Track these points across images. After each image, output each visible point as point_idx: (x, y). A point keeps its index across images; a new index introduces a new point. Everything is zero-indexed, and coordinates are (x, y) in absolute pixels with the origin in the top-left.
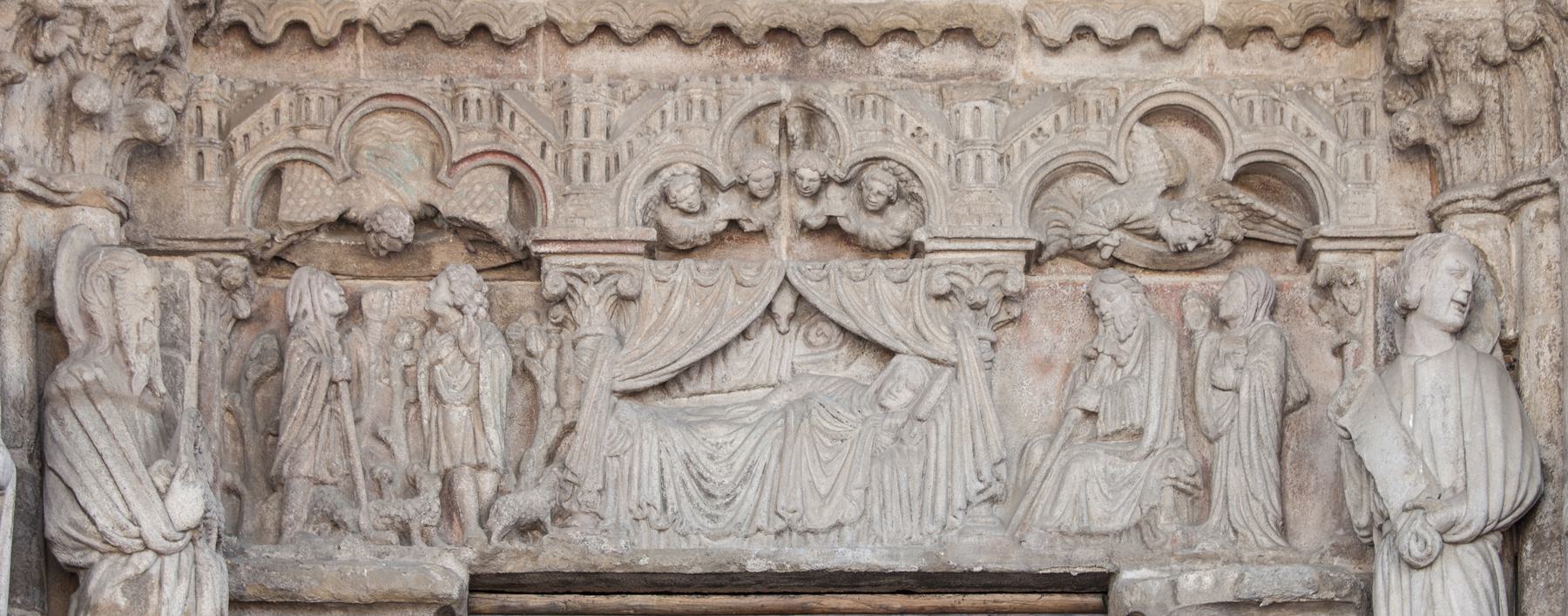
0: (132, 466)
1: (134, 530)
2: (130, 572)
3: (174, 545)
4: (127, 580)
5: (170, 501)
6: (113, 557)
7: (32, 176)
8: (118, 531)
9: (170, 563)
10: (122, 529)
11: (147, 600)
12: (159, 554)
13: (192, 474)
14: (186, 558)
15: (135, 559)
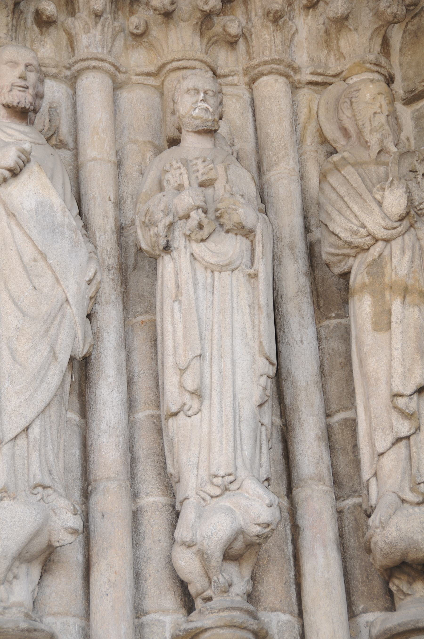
0: (361, 195)
1: (363, 231)
2: (370, 259)
3: (394, 232)
4: (369, 265)
5: (385, 204)
6: (359, 257)
7: (312, 71)
8: (355, 237)
9: (396, 245)
10: (356, 234)
11: (383, 273)
12: (387, 241)
13: (395, 182)
14: (409, 238)
15: (372, 250)
